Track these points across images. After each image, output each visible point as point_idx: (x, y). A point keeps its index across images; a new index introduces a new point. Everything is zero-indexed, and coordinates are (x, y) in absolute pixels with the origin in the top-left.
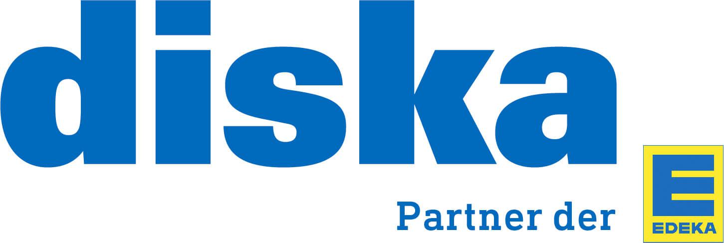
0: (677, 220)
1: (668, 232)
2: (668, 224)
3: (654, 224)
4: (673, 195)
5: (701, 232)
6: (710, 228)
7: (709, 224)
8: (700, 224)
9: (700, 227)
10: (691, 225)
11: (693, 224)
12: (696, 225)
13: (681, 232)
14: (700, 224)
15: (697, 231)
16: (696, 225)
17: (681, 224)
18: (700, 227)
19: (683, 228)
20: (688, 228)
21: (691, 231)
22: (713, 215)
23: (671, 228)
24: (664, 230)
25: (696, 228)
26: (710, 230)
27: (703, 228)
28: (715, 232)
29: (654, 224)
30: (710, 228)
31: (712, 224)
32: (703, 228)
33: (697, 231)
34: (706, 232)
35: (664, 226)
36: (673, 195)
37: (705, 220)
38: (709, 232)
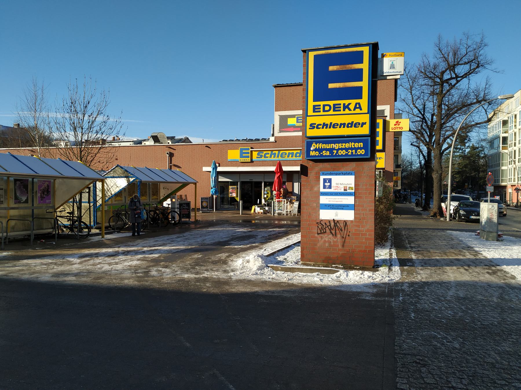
0: (331, 103)
1: (324, 111)
2: (324, 106)
3: (314, 106)
4: (329, 85)
5: (350, 110)
6: (358, 106)
7: (356, 104)
8: (349, 104)
9: (349, 106)
10: (342, 106)
11: (344, 104)
12: (346, 105)
13: (334, 110)
14: (349, 104)
15: (347, 110)
16: (346, 105)
17: (334, 105)
18: (349, 106)
19: (336, 108)
20: (340, 107)
21: (342, 109)
22: (361, 98)
23: (327, 108)
24: (322, 110)
25: (346, 107)
26: (358, 108)
27: (352, 107)
28: (361, 109)
29: (314, 106)
30: (358, 106)
31: (359, 104)
32: (352, 107)
33: (347, 110)
34: (354, 110)
35: (322, 107)
36: (329, 85)
37: (353, 102)
38: (356, 109)
